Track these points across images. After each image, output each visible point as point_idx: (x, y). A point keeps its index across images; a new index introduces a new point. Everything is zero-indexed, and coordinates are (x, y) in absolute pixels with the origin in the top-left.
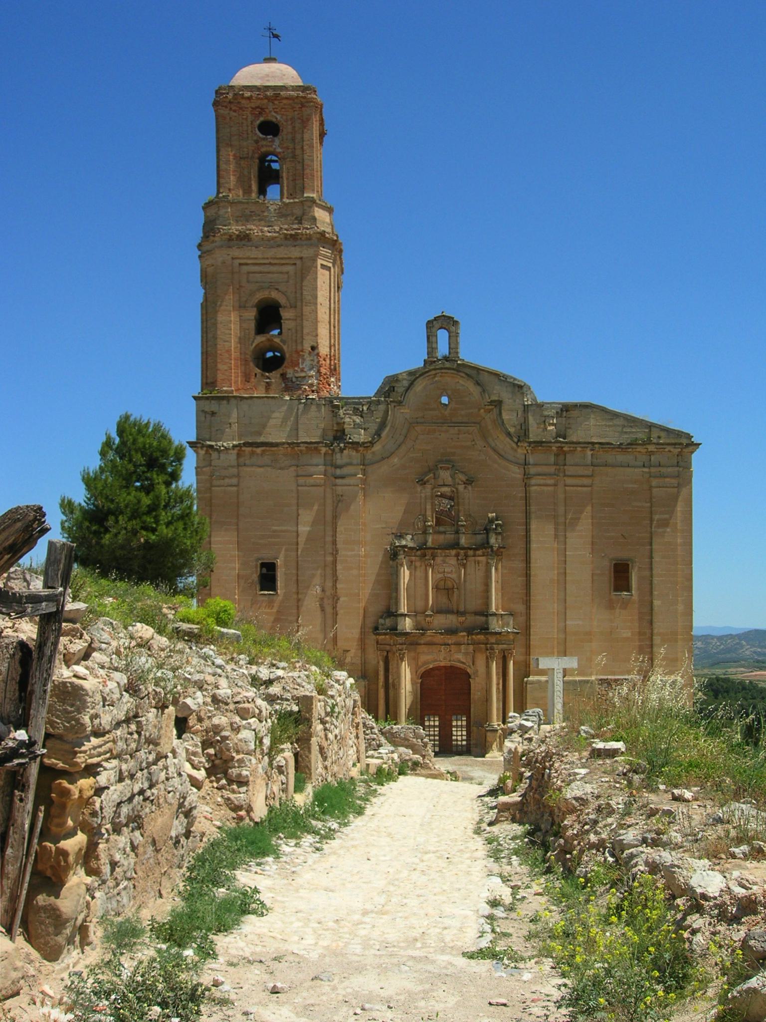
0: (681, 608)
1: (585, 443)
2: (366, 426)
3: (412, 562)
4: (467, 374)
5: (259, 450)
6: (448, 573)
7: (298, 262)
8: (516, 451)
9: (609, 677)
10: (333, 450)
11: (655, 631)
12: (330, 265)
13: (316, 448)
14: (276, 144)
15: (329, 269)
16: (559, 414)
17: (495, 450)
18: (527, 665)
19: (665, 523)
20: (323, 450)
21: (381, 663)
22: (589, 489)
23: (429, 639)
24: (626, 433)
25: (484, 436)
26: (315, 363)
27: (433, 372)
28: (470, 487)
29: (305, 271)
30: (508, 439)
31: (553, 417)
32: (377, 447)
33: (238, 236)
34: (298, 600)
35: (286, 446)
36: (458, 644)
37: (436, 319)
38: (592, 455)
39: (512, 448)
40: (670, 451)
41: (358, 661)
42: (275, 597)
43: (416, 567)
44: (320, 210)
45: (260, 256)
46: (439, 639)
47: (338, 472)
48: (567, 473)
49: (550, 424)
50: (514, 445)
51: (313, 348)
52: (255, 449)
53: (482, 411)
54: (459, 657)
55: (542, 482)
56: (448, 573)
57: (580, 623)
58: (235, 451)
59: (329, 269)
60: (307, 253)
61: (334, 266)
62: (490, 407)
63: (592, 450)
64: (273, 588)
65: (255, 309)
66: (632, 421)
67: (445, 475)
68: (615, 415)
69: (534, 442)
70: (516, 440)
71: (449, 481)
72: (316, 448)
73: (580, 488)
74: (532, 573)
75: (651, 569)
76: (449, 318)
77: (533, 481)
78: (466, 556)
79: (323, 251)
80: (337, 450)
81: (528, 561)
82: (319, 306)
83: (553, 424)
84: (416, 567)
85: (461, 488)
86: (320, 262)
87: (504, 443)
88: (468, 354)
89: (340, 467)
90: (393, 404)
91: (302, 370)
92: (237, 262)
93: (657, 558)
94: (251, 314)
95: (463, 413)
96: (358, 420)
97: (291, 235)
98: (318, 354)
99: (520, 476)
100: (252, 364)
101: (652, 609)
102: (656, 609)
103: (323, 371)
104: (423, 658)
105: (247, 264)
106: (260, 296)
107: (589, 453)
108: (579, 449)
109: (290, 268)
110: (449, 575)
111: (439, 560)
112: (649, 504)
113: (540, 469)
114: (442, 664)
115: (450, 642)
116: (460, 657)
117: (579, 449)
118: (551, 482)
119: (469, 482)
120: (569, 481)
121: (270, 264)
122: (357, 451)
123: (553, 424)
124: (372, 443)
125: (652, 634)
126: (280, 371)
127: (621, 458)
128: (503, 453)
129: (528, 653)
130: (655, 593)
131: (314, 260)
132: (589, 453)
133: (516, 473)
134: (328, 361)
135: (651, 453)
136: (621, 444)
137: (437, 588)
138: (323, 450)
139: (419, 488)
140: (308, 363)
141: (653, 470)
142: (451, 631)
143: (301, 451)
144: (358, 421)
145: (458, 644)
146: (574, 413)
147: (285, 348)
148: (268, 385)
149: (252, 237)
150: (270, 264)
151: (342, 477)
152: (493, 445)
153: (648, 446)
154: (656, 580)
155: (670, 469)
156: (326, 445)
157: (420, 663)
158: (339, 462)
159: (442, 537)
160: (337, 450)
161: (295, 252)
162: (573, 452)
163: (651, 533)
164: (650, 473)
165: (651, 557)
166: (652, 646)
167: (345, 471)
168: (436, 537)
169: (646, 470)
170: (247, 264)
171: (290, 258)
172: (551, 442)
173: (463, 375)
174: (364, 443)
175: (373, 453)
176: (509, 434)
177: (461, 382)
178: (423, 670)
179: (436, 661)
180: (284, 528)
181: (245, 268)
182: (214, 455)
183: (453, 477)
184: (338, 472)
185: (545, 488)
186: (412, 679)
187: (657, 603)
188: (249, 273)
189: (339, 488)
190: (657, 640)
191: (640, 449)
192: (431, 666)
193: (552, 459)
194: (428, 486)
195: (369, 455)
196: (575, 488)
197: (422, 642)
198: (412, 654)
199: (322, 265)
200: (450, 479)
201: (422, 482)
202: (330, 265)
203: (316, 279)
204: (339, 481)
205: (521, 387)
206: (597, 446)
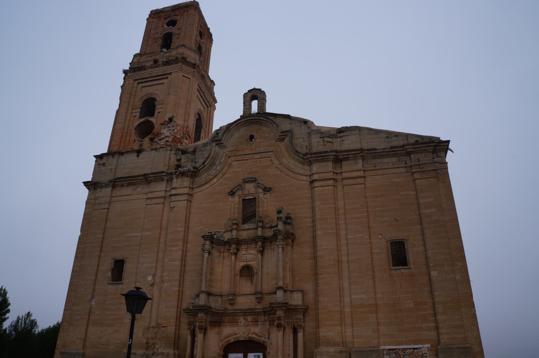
9: (397, 347)
11: (437, 300)
14: (173, 30)
21: (189, 338)
43: (224, 257)
57: (364, 296)
67: (250, 188)
71: (253, 190)
74: (319, 254)
84: (224, 257)
85: (261, 195)
88: (270, 109)
100: (134, 135)
101: (430, 280)
119: (267, 190)
120: (345, 182)
125: (434, 303)
126: (150, 136)
129: (318, 327)
130: (431, 265)
139: (230, 198)
148: (141, 145)
163: (420, 214)
165: (423, 234)
166: (435, 315)
188: (143, 87)
190: (440, 309)
201: (232, 193)
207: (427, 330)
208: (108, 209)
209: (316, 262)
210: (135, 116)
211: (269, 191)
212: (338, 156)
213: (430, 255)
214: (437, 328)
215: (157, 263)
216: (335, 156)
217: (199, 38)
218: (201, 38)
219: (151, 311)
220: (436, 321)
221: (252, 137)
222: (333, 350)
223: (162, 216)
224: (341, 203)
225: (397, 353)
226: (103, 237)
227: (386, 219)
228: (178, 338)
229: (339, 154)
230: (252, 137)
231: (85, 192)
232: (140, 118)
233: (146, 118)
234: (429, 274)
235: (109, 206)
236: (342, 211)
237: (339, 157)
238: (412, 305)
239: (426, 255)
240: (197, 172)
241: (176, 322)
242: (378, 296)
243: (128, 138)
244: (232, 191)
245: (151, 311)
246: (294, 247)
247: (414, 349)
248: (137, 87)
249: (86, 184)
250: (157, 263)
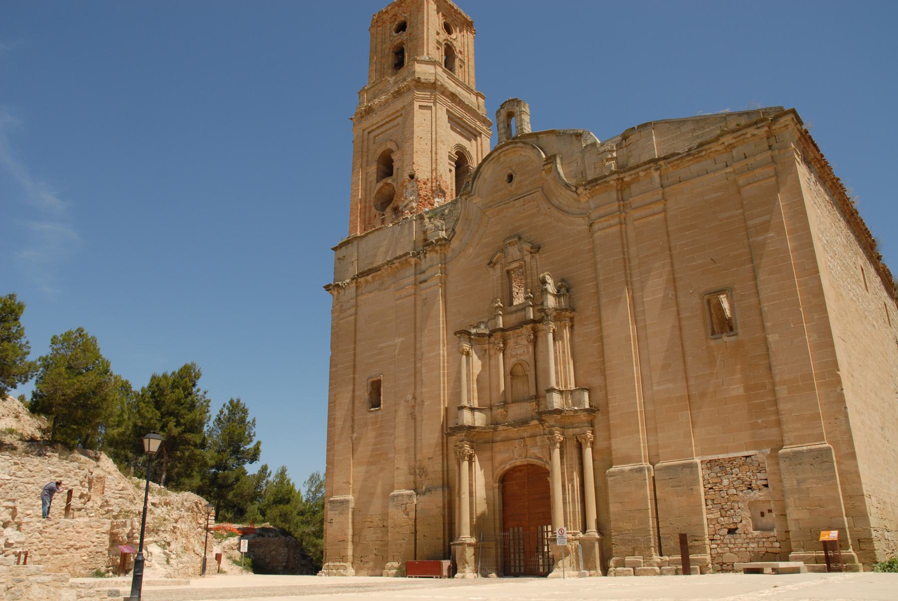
0: (809, 338)
1: (645, 164)
2: (448, 226)
3: (485, 351)
4: (523, 143)
5: (369, 278)
6: (521, 355)
7: (403, 112)
8: (579, 201)
9: (721, 456)
10: (420, 258)
11: (777, 379)
12: (432, 104)
13: (406, 260)
14: (404, 36)
15: (430, 108)
16: (619, 146)
17: (559, 209)
18: (609, 450)
19: (765, 227)
20: (413, 261)
22: (662, 215)
23: (503, 434)
24: (697, 137)
25: (547, 198)
26: (415, 188)
27: (496, 154)
28: (537, 256)
29: (406, 114)
30: (569, 192)
31: (613, 151)
32: (455, 244)
33: (365, 111)
34: (396, 411)
35: (386, 267)
36: (533, 436)
37: (502, 107)
38: (660, 176)
39: (576, 200)
40: (754, 135)
41: (438, 467)
42: (380, 413)
44: (424, 66)
45: (379, 119)
46: (514, 432)
47: (423, 277)
48: (633, 206)
49: (608, 160)
50: (575, 195)
51: (412, 177)
52: (367, 278)
53: (543, 173)
54: (535, 453)
55: (605, 224)
56: (521, 355)
57: (670, 386)
58: (354, 285)
59: (430, 108)
60: (406, 99)
61: (435, 105)
62: (549, 166)
63: (657, 169)
64: (379, 405)
65: (375, 163)
66: (701, 122)
67: (514, 251)
68: (683, 122)
69: (589, 182)
70: (574, 189)
72: (406, 260)
73: (650, 218)
74: (605, 333)
75: (758, 293)
76: (513, 100)
77: (596, 227)
78: (535, 332)
79: (418, 93)
80: (422, 256)
81: (600, 322)
82: (416, 140)
83: (612, 159)
85: (528, 258)
86: (416, 104)
87: (565, 198)
89: (424, 272)
90: (464, 197)
91: (406, 199)
92: (366, 132)
93: (762, 277)
94: (373, 169)
95: (527, 182)
96: (438, 223)
97: (397, 92)
98: (417, 180)
99: (586, 227)
100: (373, 208)
101: (768, 350)
102: (773, 347)
103: (423, 193)
104: (499, 458)
105: (373, 130)
106: (380, 152)
107: (656, 175)
108: (642, 174)
109: (400, 120)
110: (522, 358)
111: (511, 343)
112: (740, 211)
113: (602, 211)
114: (518, 463)
115: (526, 435)
116: (535, 451)
117: (642, 174)
118: (617, 220)
119: (536, 249)
121: (387, 122)
122: (436, 252)
123: (612, 159)
124: (448, 241)
125: (774, 384)
126: (391, 205)
127: (695, 167)
128: (566, 208)
130: (768, 324)
131: (411, 104)
132: (656, 175)
133: (581, 224)
134: (429, 185)
135: (731, 146)
136: (690, 150)
137: (512, 374)
138: (413, 261)
139: (491, 271)
140: (410, 190)
141: (737, 166)
142: (524, 422)
143: (397, 268)
144: (439, 224)
145: (533, 436)
146: (633, 138)
147: (394, 185)
149: (374, 107)
150: (387, 122)
151: (425, 281)
152: (556, 203)
153: (722, 140)
154: (765, 307)
155: (759, 158)
156: (414, 256)
157: (496, 464)
158: (423, 267)
159: (514, 316)
160: (422, 256)
161: (399, 104)
162: (636, 180)
164: (734, 172)
166: (775, 403)
167: (427, 274)
168: (508, 318)
169: (729, 170)
170: (373, 130)
171: (398, 111)
172: (605, 176)
173: (521, 145)
174: (437, 241)
175: (453, 250)
176: (567, 186)
177: (523, 153)
178: (499, 472)
179: (512, 459)
180: (387, 344)
181: (372, 134)
182: (342, 292)
183: (521, 250)
184: (423, 277)
185: (609, 230)
186: (486, 484)
187: (772, 338)
188: (375, 137)
189: (424, 292)
190: (782, 391)
191: (715, 147)
192: (508, 467)
193: (614, 195)
194: (498, 266)
195: (449, 254)
196: (645, 220)
197: (499, 439)
198: (488, 454)
199: (421, 107)
200: (518, 253)
201: (491, 264)
202: (432, 104)
203: (413, 120)
204: (423, 285)
205: (579, 136)
206: (661, 163)
207: (765, 427)
208: (356, 314)
209: (603, 345)
210: (371, 182)
211: (538, 251)
212: (622, 179)
213: (766, 309)
214: (779, 423)
215: (415, 377)
216: (618, 179)
217: (444, 35)
218: (449, 32)
219: (415, 439)
220: (777, 412)
221: (510, 178)
222: (629, 468)
223: (415, 313)
224: (633, 250)
225: (722, 467)
226: (355, 354)
227: (700, 262)
228: (448, 471)
229: (622, 176)
230: (510, 178)
231: (328, 298)
232: (377, 182)
233: (384, 180)
234: (766, 339)
235: (356, 310)
236: (635, 262)
237: (626, 179)
238: (741, 391)
239: (761, 309)
240: (444, 245)
241: (443, 450)
242: (692, 382)
243: (367, 214)
244: (491, 262)
245: (415, 439)
246: (576, 327)
247: (747, 457)
248: (368, 139)
249: (327, 288)
250: (415, 377)
